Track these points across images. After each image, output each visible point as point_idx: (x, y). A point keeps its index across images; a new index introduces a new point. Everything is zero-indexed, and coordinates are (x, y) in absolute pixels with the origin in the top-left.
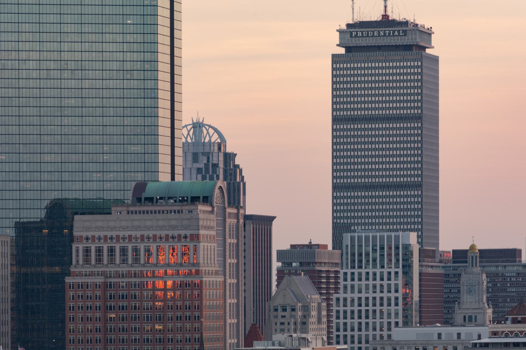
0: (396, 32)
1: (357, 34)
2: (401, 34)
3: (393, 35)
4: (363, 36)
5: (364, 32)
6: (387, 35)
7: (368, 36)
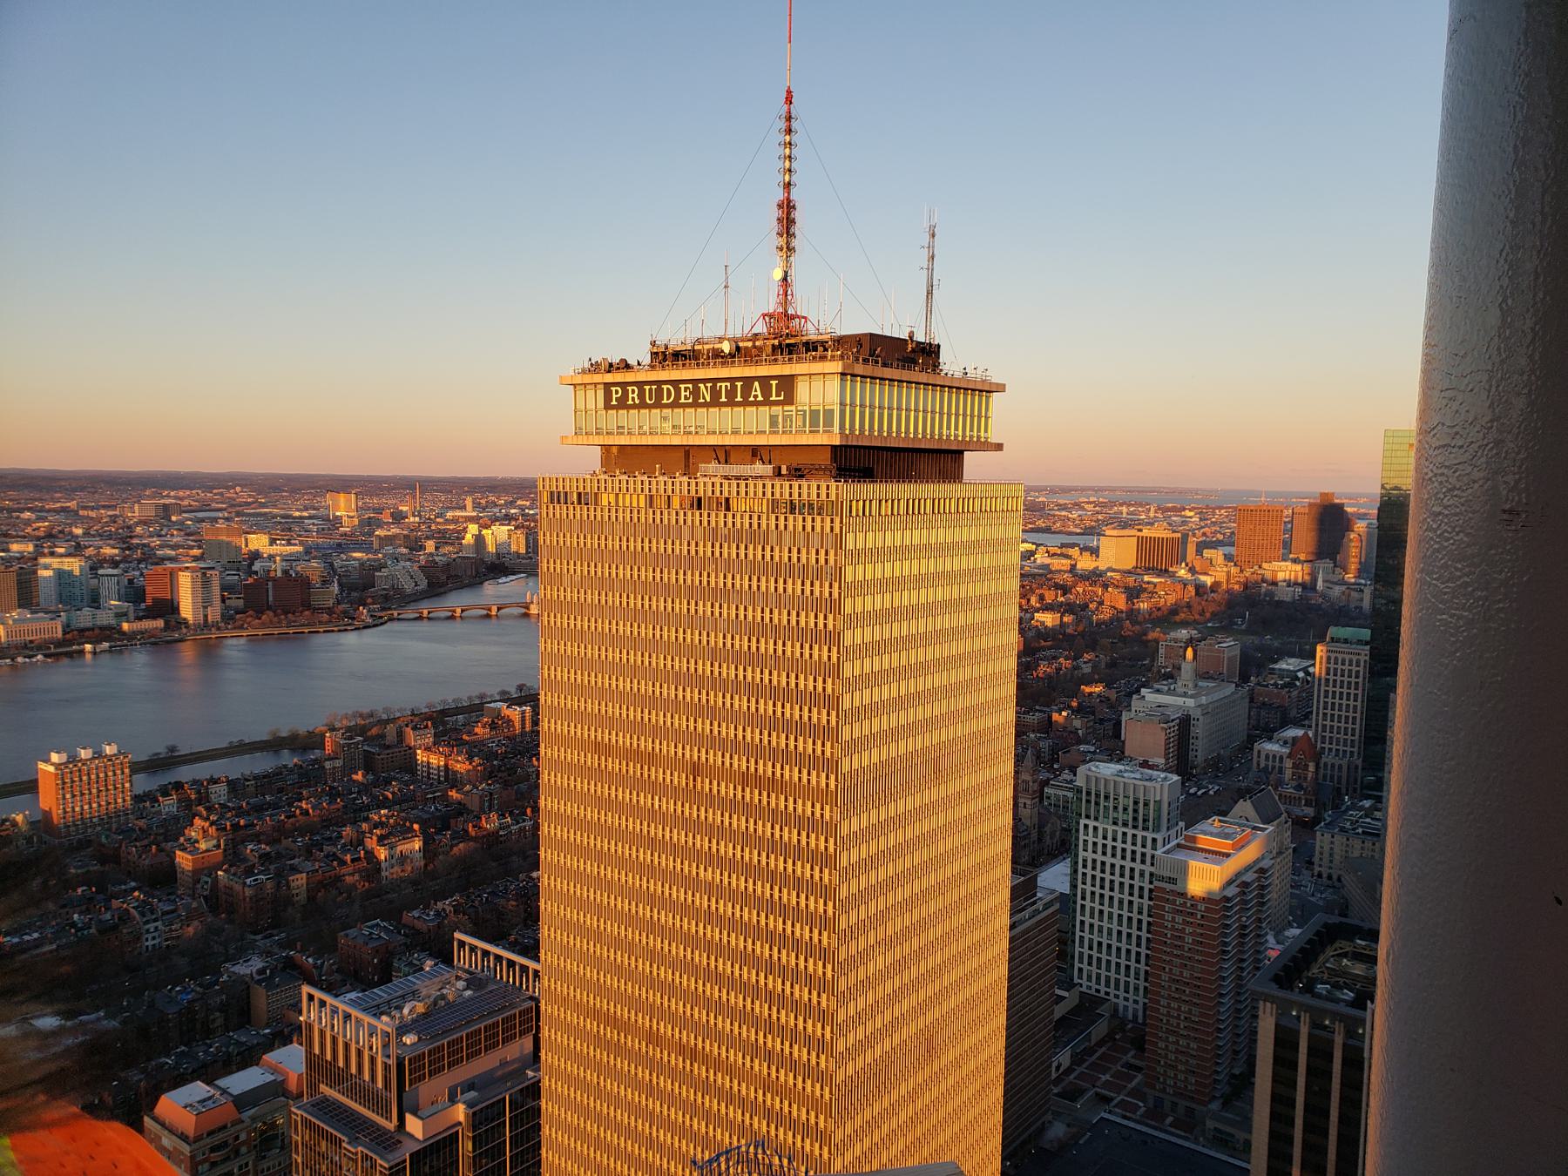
0: (756, 384)
1: (625, 393)
2: (774, 398)
3: (745, 403)
4: (643, 405)
5: (647, 388)
6: (723, 399)
7: (658, 405)
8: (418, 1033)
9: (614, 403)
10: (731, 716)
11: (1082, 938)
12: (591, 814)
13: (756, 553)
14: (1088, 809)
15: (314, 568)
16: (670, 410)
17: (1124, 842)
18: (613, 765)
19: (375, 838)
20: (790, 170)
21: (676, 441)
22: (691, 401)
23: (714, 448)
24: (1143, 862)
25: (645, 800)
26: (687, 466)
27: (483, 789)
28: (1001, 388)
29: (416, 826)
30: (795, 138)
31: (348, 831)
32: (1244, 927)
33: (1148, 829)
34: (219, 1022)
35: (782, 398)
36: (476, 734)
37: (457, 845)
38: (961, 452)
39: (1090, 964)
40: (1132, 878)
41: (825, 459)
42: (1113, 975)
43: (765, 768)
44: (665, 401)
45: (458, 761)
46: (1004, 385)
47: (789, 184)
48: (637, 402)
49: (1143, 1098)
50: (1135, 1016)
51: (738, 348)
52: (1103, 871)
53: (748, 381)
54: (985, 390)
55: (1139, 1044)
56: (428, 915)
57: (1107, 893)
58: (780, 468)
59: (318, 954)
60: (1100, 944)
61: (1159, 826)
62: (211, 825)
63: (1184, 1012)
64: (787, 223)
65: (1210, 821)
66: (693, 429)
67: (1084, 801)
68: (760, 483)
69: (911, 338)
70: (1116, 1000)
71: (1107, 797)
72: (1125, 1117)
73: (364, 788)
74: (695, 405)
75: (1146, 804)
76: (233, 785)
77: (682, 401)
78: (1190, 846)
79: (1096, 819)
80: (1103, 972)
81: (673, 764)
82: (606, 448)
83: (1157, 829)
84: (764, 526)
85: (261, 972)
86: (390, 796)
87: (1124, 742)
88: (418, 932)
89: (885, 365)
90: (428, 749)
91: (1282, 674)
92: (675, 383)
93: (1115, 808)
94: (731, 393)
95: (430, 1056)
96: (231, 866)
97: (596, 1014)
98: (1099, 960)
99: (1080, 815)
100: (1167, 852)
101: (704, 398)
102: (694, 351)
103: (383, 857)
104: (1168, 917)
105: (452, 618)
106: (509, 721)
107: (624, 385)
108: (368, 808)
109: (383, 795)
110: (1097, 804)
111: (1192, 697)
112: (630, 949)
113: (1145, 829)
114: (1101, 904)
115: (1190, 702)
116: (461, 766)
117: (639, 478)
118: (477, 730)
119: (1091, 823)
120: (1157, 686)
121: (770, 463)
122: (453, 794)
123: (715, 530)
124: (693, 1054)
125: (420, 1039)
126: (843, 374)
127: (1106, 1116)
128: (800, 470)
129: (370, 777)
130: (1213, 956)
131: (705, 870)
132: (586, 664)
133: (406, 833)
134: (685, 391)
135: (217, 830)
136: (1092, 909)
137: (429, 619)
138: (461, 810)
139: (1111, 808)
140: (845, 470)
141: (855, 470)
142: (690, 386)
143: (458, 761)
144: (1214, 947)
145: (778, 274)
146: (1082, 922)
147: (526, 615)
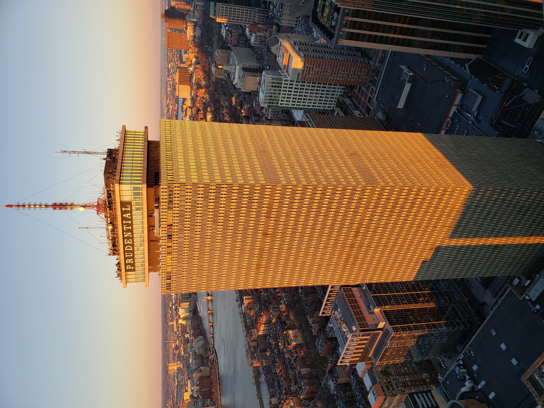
0: (124, 216)
1: (128, 264)
2: (129, 209)
3: (131, 220)
4: (133, 257)
5: (126, 256)
6: (130, 228)
7: (133, 252)
8: (352, 326)
9: (132, 268)
10: (247, 222)
11: (318, 106)
12: (280, 269)
13: (188, 215)
14: (275, 103)
15: (196, 375)
16: (135, 247)
17: (286, 91)
18: (264, 263)
19: (289, 346)
20: (40, 205)
21: (146, 245)
22: (131, 240)
23: (149, 231)
24: (292, 85)
25: (275, 251)
26: (156, 241)
27: (272, 311)
28: (124, 127)
29: (285, 333)
30: (27, 203)
31: (287, 356)
32: (314, 50)
33: (281, 83)
34: (349, 393)
35: (129, 206)
36: (253, 314)
37: (290, 318)
38: (148, 141)
39: (326, 104)
40: (298, 89)
41: (152, 190)
42: (330, 96)
43: (264, 210)
44: (131, 249)
45: (262, 320)
46: (123, 126)
47: (45, 205)
48: (132, 259)
49: (369, 87)
50: (343, 89)
51: (111, 223)
52: (296, 99)
53: (123, 219)
54: (125, 133)
55: (352, 87)
56: (314, 326)
57: (303, 97)
58: (156, 206)
59: (327, 362)
60: (320, 100)
61: (280, 79)
62: (285, 402)
63: (342, 72)
64: (62, 206)
65: (278, 61)
66: (142, 239)
67: (272, 104)
68: (162, 214)
69: (105, 159)
70: (338, 95)
71: (271, 97)
72: (375, 93)
73: (272, 351)
74: (132, 238)
75: (273, 83)
76: (272, 396)
77: (131, 243)
78: (287, 67)
79: (278, 100)
80: (329, 99)
81: (263, 242)
82: (150, 270)
83: (281, 80)
84: (178, 212)
85: (333, 380)
86: (275, 342)
87: (252, 91)
88: (319, 329)
89: (116, 169)
90: (258, 331)
91: (227, 35)
92: (125, 246)
93: (275, 94)
94: (128, 225)
95: (359, 321)
96: (299, 394)
97: (345, 265)
98: (325, 101)
99: (277, 106)
100: (289, 76)
101: (130, 235)
102: (112, 239)
103: (295, 343)
104: (310, 76)
105: (213, 326)
106: (249, 303)
107: (126, 265)
108: (279, 350)
109: (274, 345)
110: (273, 100)
111: (236, 67)
112: (324, 254)
113: (281, 83)
114: (307, 99)
115: (238, 67)
116: (264, 319)
117: (161, 258)
118: (252, 315)
119: (280, 102)
120: (232, 79)
121: (154, 210)
122: (274, 321)
123: (180, 230)
124: (357, 232)
125: (354, 325)
126: (120, 183)
127: (375, 99)
128: (156, 199)
129: (268, 350)
130: (323, 61)
131: (298, 230)
132: (229, 275)
133: (287, 336)
134: (127, 242)
135: (287, 400)
136: (308, 103)
137: (213, 334)
138: (279, 318)
139: (275, 95)
140: (156, 183)
141: (156, 179)
142: (125, 240)
143: (262, 320)
144: (320, 61)
145: (82, 209)
146: (313, 106)
147: (211, 300)
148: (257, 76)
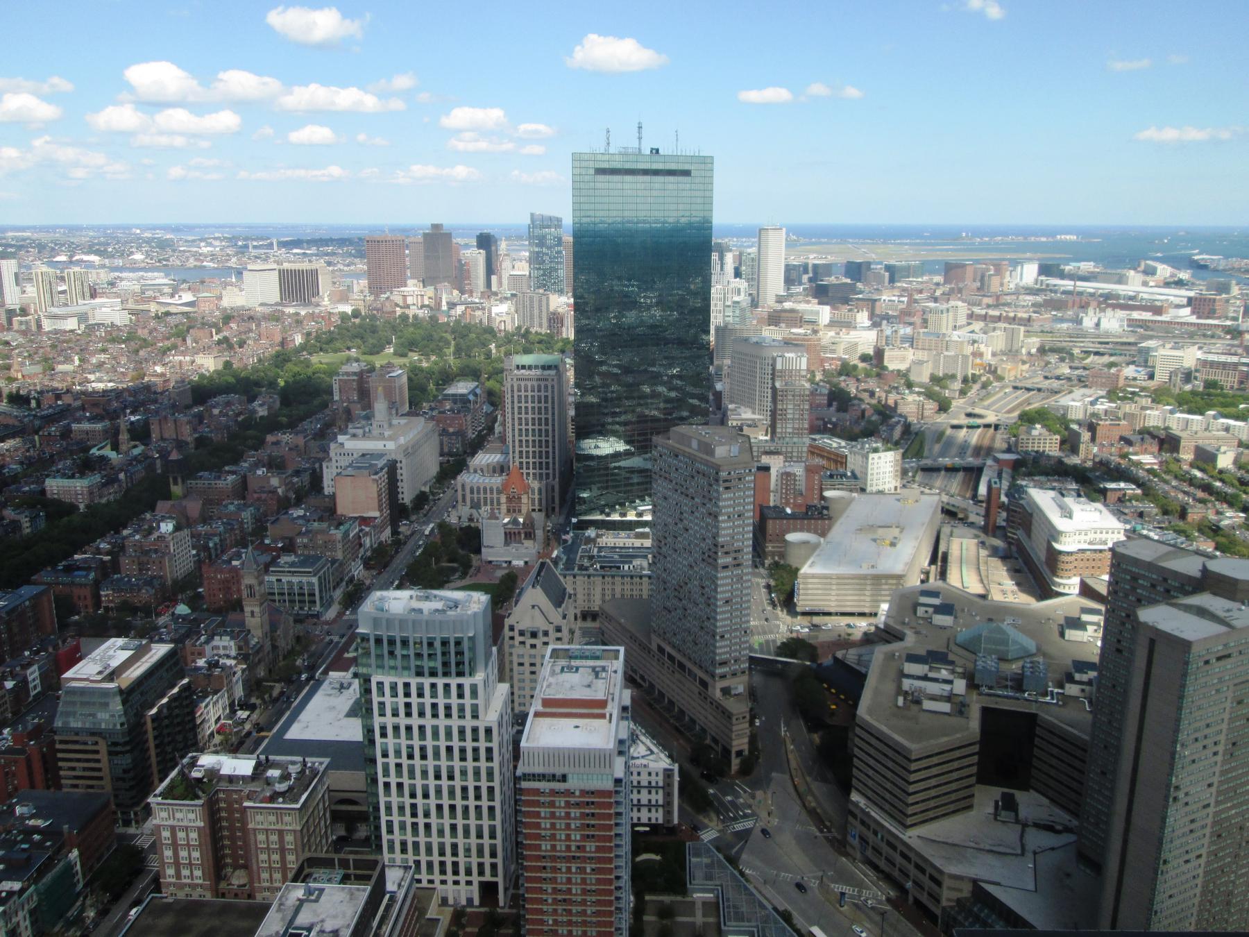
87: (333, 497)
91: (456, 398)
111: (390, 438)
148: (381, 511)
